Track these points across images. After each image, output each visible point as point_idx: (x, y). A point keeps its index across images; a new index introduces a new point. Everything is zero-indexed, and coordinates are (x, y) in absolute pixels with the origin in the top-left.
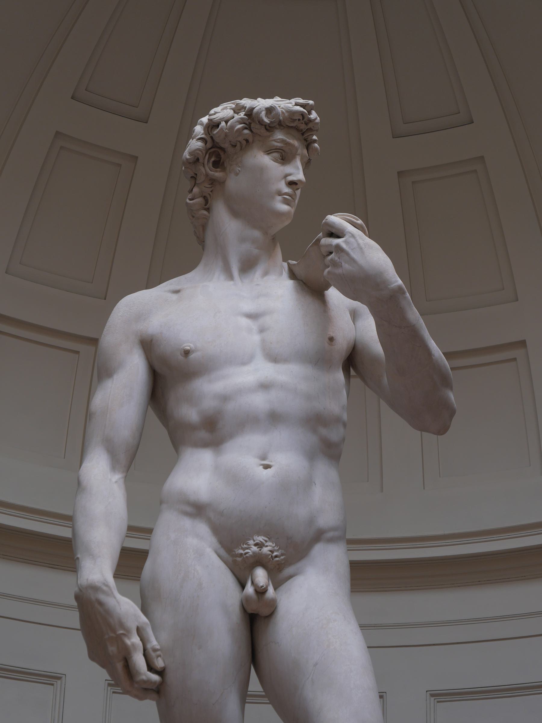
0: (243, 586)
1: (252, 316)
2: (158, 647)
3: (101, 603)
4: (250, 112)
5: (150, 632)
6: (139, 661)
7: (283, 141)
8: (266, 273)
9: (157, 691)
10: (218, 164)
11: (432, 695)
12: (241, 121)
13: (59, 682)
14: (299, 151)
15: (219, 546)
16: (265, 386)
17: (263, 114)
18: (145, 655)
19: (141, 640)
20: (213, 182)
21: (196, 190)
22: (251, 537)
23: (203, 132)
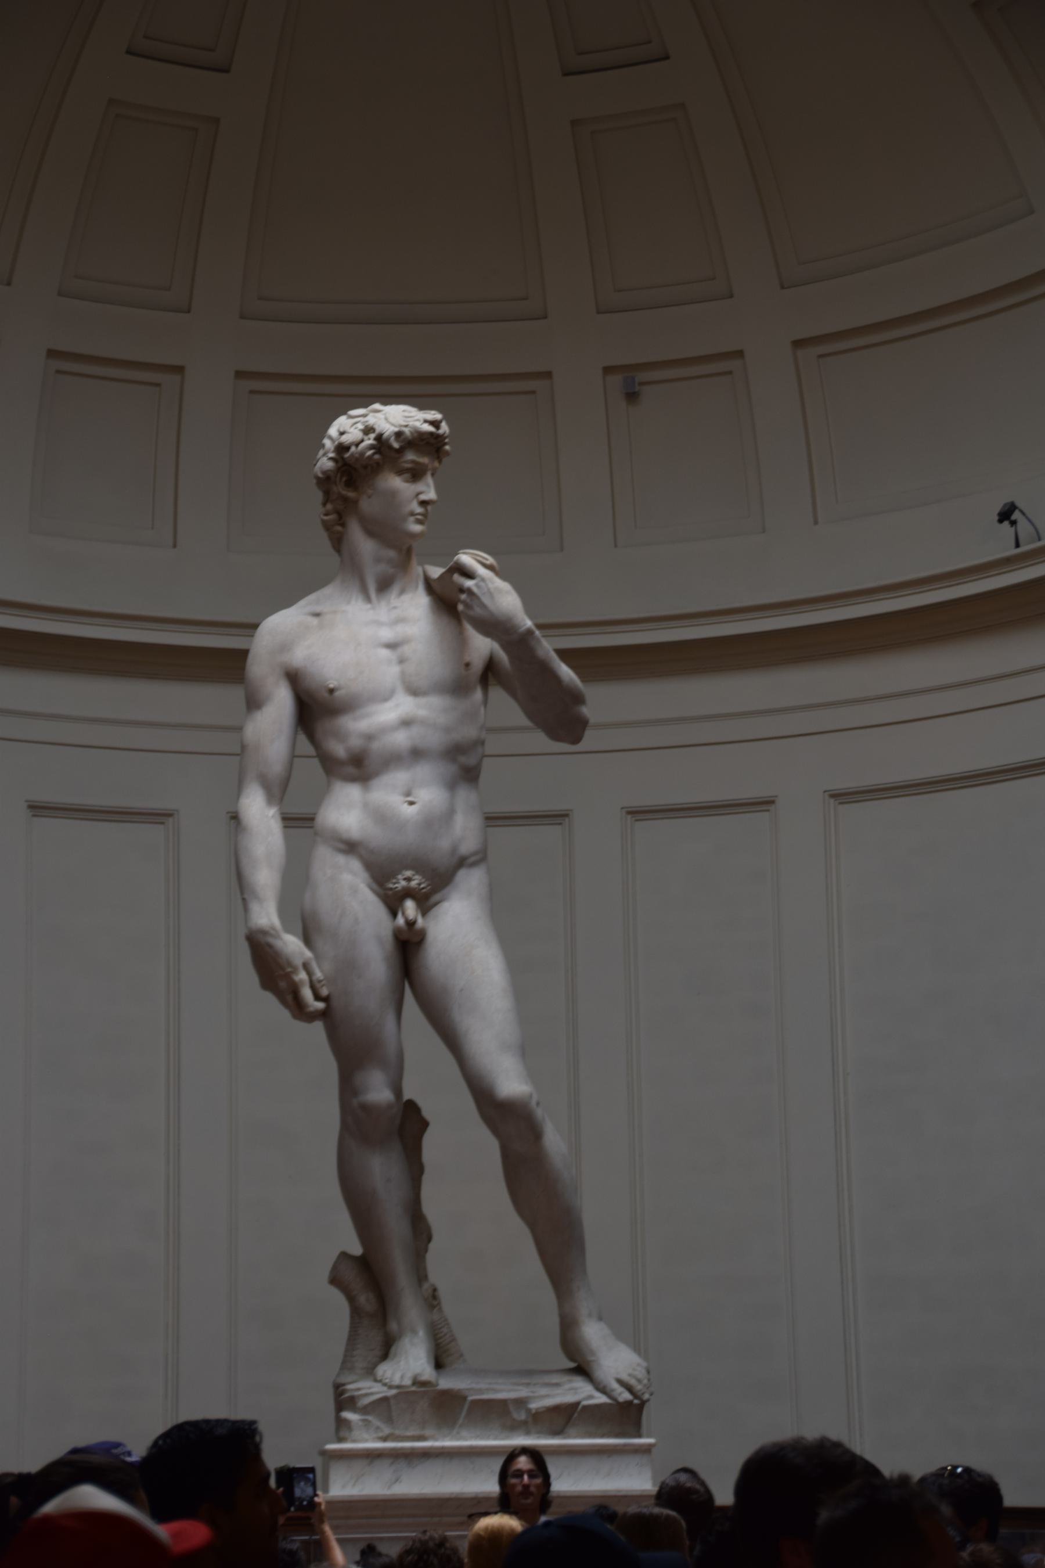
0: (394, 914)
1: (392, 646)
2: (322, 978)
3: (270, 946)
4: (379, 438)
5: (314, 965)
6: (307, 994)
7: (413, 462)
8: (402, 592)
9: (324, 1015)
10: (351, 483)
11: (629, 813)
12: (371, 447)
13: (171, 819)
14: (430, 467)
15: (370, 881)
16: (406, 723)
17: (393, 438)
18: (313, 987)
19: (310, 973)
20: (345, 499)
21: (329, 506)
22: (399, 872)
23: (332, 449)
